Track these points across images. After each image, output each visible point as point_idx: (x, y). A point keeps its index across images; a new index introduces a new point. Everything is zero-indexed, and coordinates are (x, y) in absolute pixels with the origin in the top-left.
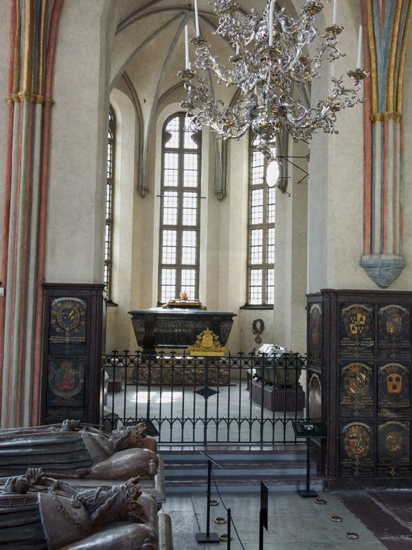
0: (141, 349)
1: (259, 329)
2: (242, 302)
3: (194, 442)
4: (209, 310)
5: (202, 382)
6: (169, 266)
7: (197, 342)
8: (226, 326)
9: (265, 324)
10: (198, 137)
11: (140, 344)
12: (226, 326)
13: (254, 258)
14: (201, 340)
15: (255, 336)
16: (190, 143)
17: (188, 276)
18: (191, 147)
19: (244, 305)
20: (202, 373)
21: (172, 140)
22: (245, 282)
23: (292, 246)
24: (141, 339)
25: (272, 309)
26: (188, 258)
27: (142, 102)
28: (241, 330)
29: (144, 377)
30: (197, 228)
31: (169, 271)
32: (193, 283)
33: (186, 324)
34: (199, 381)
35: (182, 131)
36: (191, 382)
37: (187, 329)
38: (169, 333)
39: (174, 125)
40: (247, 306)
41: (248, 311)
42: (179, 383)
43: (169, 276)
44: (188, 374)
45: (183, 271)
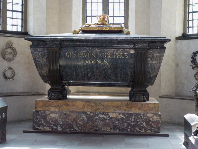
0: (48, 87)
5: (123, 129)
11: (45, 79)
22: (182, 8)
28: (177, 65)
32: (122, 13)
33: (100, 52)
34: (119, 129)
36: (107, 129)
38: (79, 66)
40: (185, 37)
41: (186, 42)
42: (93, 131)
44: (104, 119)
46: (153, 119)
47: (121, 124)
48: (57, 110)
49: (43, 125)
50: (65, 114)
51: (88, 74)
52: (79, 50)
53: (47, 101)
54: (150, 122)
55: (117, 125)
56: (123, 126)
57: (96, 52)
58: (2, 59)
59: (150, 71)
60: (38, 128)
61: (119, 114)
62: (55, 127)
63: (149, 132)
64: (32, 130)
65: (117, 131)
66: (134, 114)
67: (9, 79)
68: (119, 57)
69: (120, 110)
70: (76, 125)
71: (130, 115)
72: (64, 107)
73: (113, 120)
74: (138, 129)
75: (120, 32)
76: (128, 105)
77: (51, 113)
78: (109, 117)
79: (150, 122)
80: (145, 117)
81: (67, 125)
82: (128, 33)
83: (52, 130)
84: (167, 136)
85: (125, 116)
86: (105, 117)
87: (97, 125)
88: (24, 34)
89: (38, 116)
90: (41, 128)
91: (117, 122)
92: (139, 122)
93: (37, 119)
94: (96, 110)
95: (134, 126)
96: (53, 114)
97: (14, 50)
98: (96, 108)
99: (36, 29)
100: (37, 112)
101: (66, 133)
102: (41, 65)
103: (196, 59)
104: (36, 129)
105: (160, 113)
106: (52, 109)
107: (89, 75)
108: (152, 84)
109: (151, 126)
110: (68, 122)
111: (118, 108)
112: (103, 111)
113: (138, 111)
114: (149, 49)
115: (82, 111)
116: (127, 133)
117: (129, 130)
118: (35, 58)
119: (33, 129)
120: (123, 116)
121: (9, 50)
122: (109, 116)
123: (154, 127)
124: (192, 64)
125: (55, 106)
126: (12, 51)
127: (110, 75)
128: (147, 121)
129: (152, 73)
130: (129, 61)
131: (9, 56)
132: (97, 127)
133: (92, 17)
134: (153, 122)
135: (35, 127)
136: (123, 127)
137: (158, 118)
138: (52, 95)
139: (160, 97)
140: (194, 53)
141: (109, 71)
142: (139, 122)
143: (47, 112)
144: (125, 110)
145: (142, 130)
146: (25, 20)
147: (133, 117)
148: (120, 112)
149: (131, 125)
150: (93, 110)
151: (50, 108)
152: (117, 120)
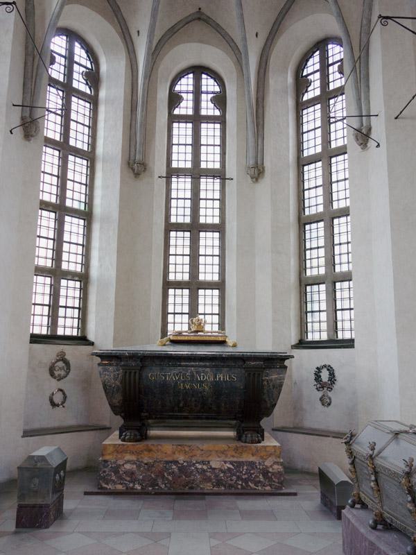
0: (119, 421)
1: (325, 381)
2: (294, 341)
4: (244, 348)
5: (231, 486)
8: (274, 377)
9: (336, 374)
10: (220, 100)
12: (274, 377)
13: (311, 268)
15: (320, 394)
16: (208, 108)
17: (208, 299)
18: (210, 113)
19: (297, 342)
20: (229, 468)
21: (183, 104)
23: (392, 229)
24: (115, 401)
25: (352, 346)
26: (209, 272)
27: (134, 35)
29: (120, 478)
30: (219, 228)
33: (197, 372)
35: (197, 92)
36: (208, 487)
37: (202, 382)
39: (186, 84)
42: (186, 490)
43: (178, 300)
44: (204, 471)
46: (273, 469)
47: (227, 478)
48: (134, 458)
49: (113, 481)
50: (146, 464)
51: (179, 402)
52: (168, 369)
53: (119, 445)
54: (270, 474)
55: (222, 480)
56: (231, 480)
57: (192, 372)
58: (50, 377)
59: (267, 399)
60: (106, 486)
61: (225, 462)
62: (131, 485)
63: (268, 488)
64: (97, 490)
65: (223, 488)
66: (246, 462)
67: (58, 405)
68: (224, 379)
69: (226, 456)
70: (163, 480)
71: (240, 464)
72: (145, 453)
73: (217, 471)
74: (252, 485)
75: (223, 343)
76: (237, 450)
77: (126, 463)
78: (211, 468)
79: (270, 474)
80: (261, 467)
81: (149, 481)
83: (127, 488)
84: (295, 494)
85: (233, 465)
86: (205, 467)
87: (193, 480)
88: (82, 340)
89: (106, 467)
90: (110, 486)
91: (222, 475)
92: (254, 473)
93: (104, 472)
94: (192, 457)
95: (246, 481)
96: (129, 465)
97: (67, 363)
98: (191, 454)
99: (103, 335)
100: (106, 461)
101: (148, 494)
102: (113, 391)
103: (320, 376)
104: (102, 488)
105: (282, 461)
106: (128, 457)
107: (181, 405)
108: (268, 415)
109: (270, 479)
110: (151, 476)
111: (223, 453)
112: (200, 459)
113: (252, 459)
114: (264, 368)
115: (170, 459)
116: (237, 491)
117: (239, 487)
118: (105, 382)
119: (99, 489)
120: (231, 466)
121: (61, 364)
122: (211, 466)
123: (274, 481)
124: (316, 383)
125: (132, 453)
126: (64, 365)
127: (211, 404)
128: (265, 473)
129: (269, 402)
130: (238, 385)
131: (59, 372)
132: (193, 483)
133: (176, 315)
134: (273, 474)
135: (101, 486)
136: (230, 482)
137: (280, 467)
138: (126, 435)
139: (273, 430)
140: (317, 368)
141: (210, 399)
142: (254, 473)
143: (120, 462)
144: (233, 456)
145: (258, 486)
146: (83, 319)
147: (245, 467)
148: (227, 460)
149: (242, 479)
150: (187, 456)
151: (124, 455)
152: (221, 470)
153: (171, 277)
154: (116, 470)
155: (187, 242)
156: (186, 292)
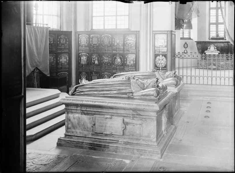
3: (208, 84)
6: (213, 24)
7: (208, 49)
14: (210, 48)
31: (213, 25)
43: (213, 28)
45: (219, 25)
82: (226, 39)
88: (190, 39)
97: (187, 45)
121: (186, 45)
143: (201, 63)
153: (211, 22)
154: (201, 65)
155: (215, 28)
156: (215, 25)
